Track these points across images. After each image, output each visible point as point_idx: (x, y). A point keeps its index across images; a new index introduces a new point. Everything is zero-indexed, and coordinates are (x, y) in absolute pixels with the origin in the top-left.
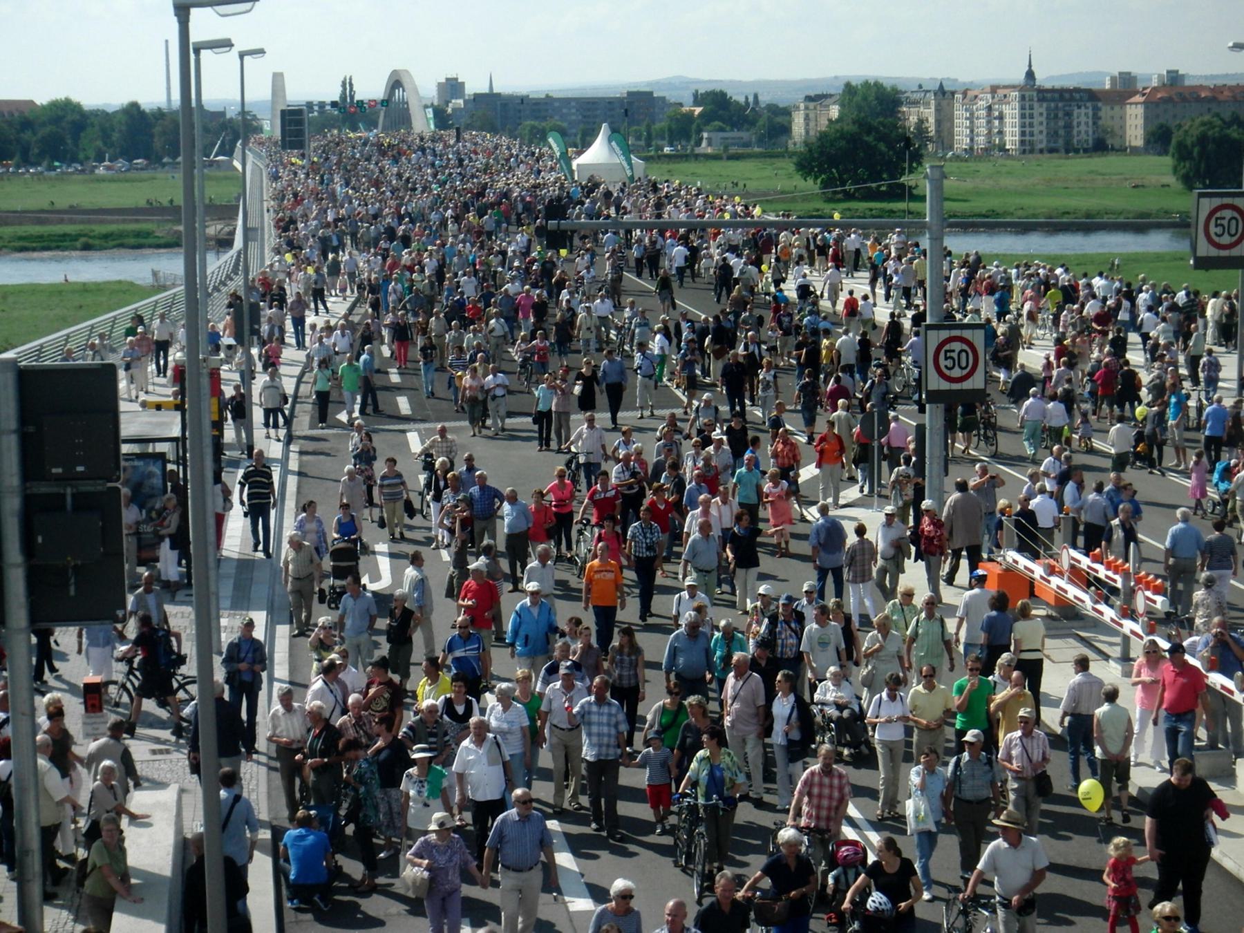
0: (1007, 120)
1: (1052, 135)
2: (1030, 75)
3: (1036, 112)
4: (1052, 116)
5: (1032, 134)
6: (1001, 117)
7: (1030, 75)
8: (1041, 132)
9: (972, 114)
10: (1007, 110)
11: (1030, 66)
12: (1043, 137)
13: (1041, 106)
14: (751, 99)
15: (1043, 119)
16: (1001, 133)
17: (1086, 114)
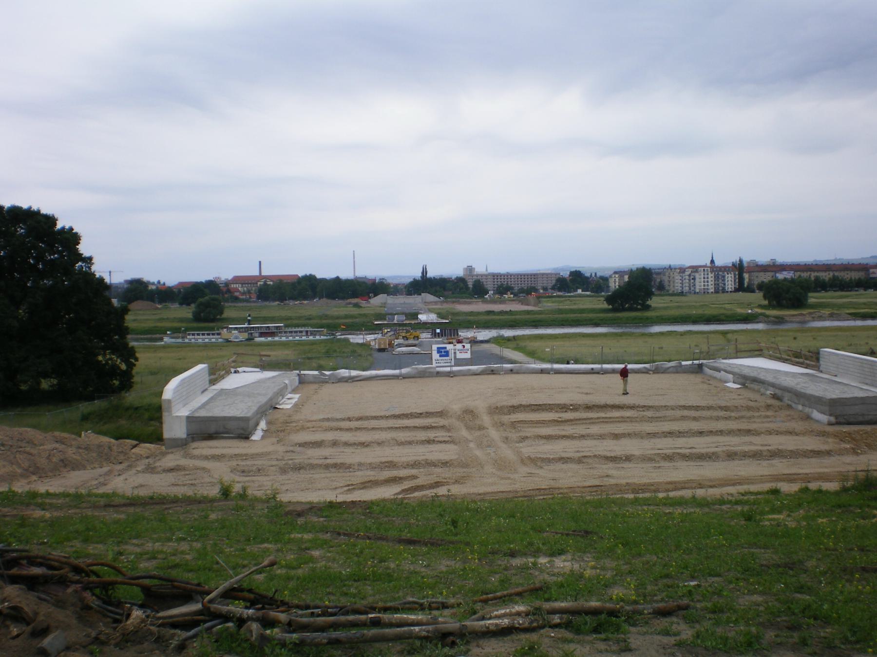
0: (697, 280)
1: (716, 285)
2: (712, 262)
4: (717, 278)
5: (708, 285)
6: (694, 279)
7: (712, 262)
9: (682, 277)
10: (697, 275)
11: (712, 258)
12: (713, 286)
13: (712, 273)
14: (593, 275)
15: (713, 279)
16: (694, 285)
17: (731, 277)
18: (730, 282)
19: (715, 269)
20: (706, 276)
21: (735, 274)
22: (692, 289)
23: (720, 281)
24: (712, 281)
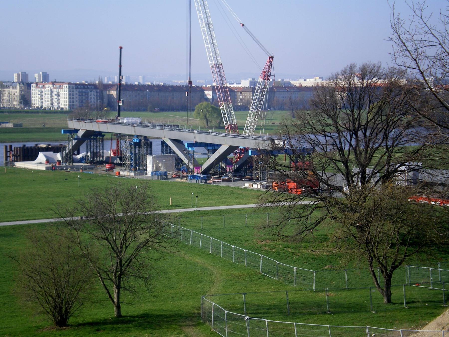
0: (61, 96)
1: (81, 102)
3: (74, 93)
5: (73, 102)
6: (58, 95)
8: (77, 101)
9: (42, 92)
13: (76, 91)
15: (77, 96)
17: (94, 94)
18: (93, 100)
19: (79, 87)
20: (71, 93)
21: (97, 92)
22: (55, 104)
23: (84, 98)
24: (77, 98)
